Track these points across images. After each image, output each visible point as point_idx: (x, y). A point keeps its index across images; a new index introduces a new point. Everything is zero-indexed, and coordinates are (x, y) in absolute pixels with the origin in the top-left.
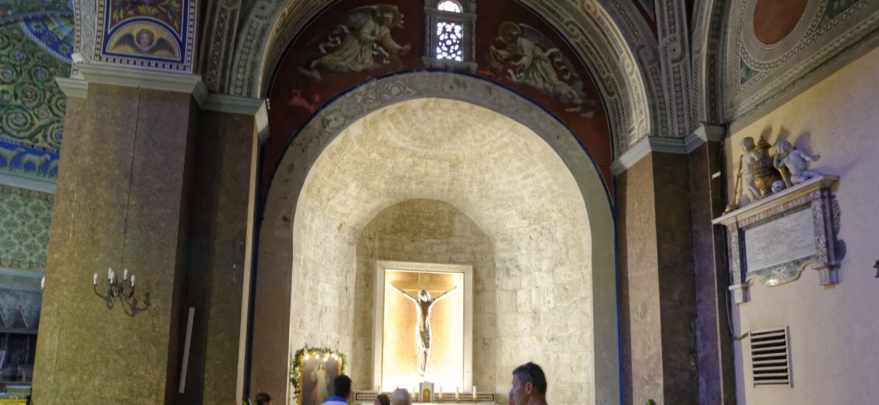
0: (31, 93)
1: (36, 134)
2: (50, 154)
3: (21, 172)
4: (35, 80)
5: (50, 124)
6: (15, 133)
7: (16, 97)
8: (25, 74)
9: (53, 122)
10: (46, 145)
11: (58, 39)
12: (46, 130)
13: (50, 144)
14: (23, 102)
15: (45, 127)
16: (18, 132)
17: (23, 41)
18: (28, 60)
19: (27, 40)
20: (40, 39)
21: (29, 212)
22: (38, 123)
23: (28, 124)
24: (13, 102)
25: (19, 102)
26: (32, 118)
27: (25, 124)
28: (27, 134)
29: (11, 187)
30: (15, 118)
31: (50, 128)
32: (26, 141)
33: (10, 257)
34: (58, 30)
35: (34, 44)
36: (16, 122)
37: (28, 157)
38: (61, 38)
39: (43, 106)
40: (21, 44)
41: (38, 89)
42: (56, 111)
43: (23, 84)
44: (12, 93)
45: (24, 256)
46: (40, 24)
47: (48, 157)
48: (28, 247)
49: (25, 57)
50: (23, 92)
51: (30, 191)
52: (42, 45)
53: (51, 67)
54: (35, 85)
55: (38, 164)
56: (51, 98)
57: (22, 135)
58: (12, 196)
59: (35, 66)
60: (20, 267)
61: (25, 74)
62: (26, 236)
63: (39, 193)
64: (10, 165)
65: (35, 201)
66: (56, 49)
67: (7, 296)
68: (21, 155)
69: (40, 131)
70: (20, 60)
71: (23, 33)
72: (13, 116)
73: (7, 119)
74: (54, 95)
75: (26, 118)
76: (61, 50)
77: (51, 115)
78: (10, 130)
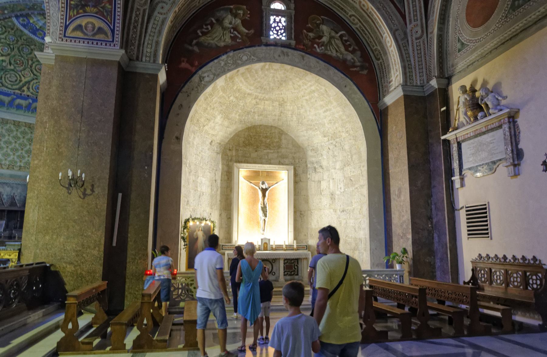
0: (20, 61)
1: (23, 87)
2: (32, 99)
3: (14, 110)
4: (22, 53)
5: (32, 81)
6: (10, 86)
7: (10, 64)
8: (16, 50)
9: (33, 79)
10: (29, 94)
11: (36, 28)
12: (29, 84)
13: (32, 93)
14: (15, 67)
15: (29, 82)
16: (12, 85)
17: (14, 30)
18: (17, 41)
19: (17, 29)
20: (25, 28)
21: (19, 135)
22: (24, 80)
23: (18, 81)
24: (9, 67)
25: (12, 67)
26: (20, 77)
27: (16, 81)
28: (17, 87)
29: (8, 120)
30: (10, 77)
31: (32, 83)
32: (17, 91)
33: (7, 163)
34: (36, 23)
35: (21, 31)
36: (10, 79)
37: (18, 101)
38: (38, 28)
39: (27, 70)
40: (13, 31)
41: (24, 59)
42: (35, 72)
43: (14, 56)
44: (8, 61)
45: (16, 162)
46: (25, 19)
47: (31, 101)
48: (19, 157)
49: (16, 39)
50: (14, 61)
51: (19, 122)
52: (26, 31)
53: (32, 45)
54: (22, 57)
55: (24, 105)
56: (32, 65)
57: (14, 87)
58: (8, 125)
59: (22, 45)
60: (14, 169)
61: (16, 50)
62: (17, 150)
63: (25, 123)
64: (7, 106)
65: (23, 128)
66: (35, 34)
67: (6, 187)
68: (13, 100)
69: (25, 85)
70: (13, 41)
71: (14, 25)
72: (8, 76)
73: (5, 78)
74: (34, 63)
75: (17, 77)
76: (38, 35)
77: (32, 75)
78: (7, 84)
